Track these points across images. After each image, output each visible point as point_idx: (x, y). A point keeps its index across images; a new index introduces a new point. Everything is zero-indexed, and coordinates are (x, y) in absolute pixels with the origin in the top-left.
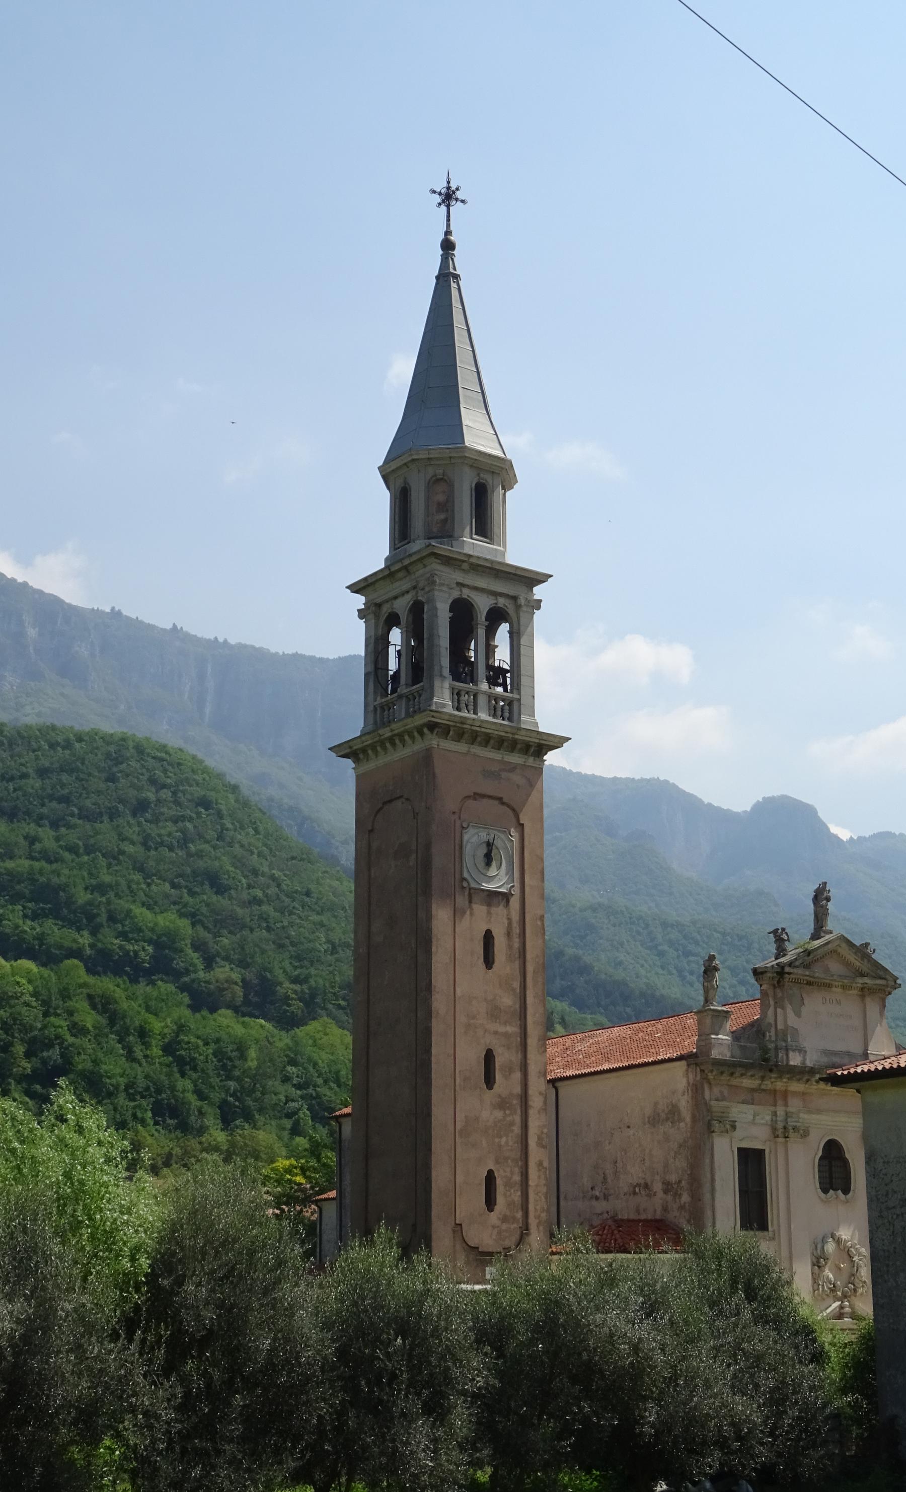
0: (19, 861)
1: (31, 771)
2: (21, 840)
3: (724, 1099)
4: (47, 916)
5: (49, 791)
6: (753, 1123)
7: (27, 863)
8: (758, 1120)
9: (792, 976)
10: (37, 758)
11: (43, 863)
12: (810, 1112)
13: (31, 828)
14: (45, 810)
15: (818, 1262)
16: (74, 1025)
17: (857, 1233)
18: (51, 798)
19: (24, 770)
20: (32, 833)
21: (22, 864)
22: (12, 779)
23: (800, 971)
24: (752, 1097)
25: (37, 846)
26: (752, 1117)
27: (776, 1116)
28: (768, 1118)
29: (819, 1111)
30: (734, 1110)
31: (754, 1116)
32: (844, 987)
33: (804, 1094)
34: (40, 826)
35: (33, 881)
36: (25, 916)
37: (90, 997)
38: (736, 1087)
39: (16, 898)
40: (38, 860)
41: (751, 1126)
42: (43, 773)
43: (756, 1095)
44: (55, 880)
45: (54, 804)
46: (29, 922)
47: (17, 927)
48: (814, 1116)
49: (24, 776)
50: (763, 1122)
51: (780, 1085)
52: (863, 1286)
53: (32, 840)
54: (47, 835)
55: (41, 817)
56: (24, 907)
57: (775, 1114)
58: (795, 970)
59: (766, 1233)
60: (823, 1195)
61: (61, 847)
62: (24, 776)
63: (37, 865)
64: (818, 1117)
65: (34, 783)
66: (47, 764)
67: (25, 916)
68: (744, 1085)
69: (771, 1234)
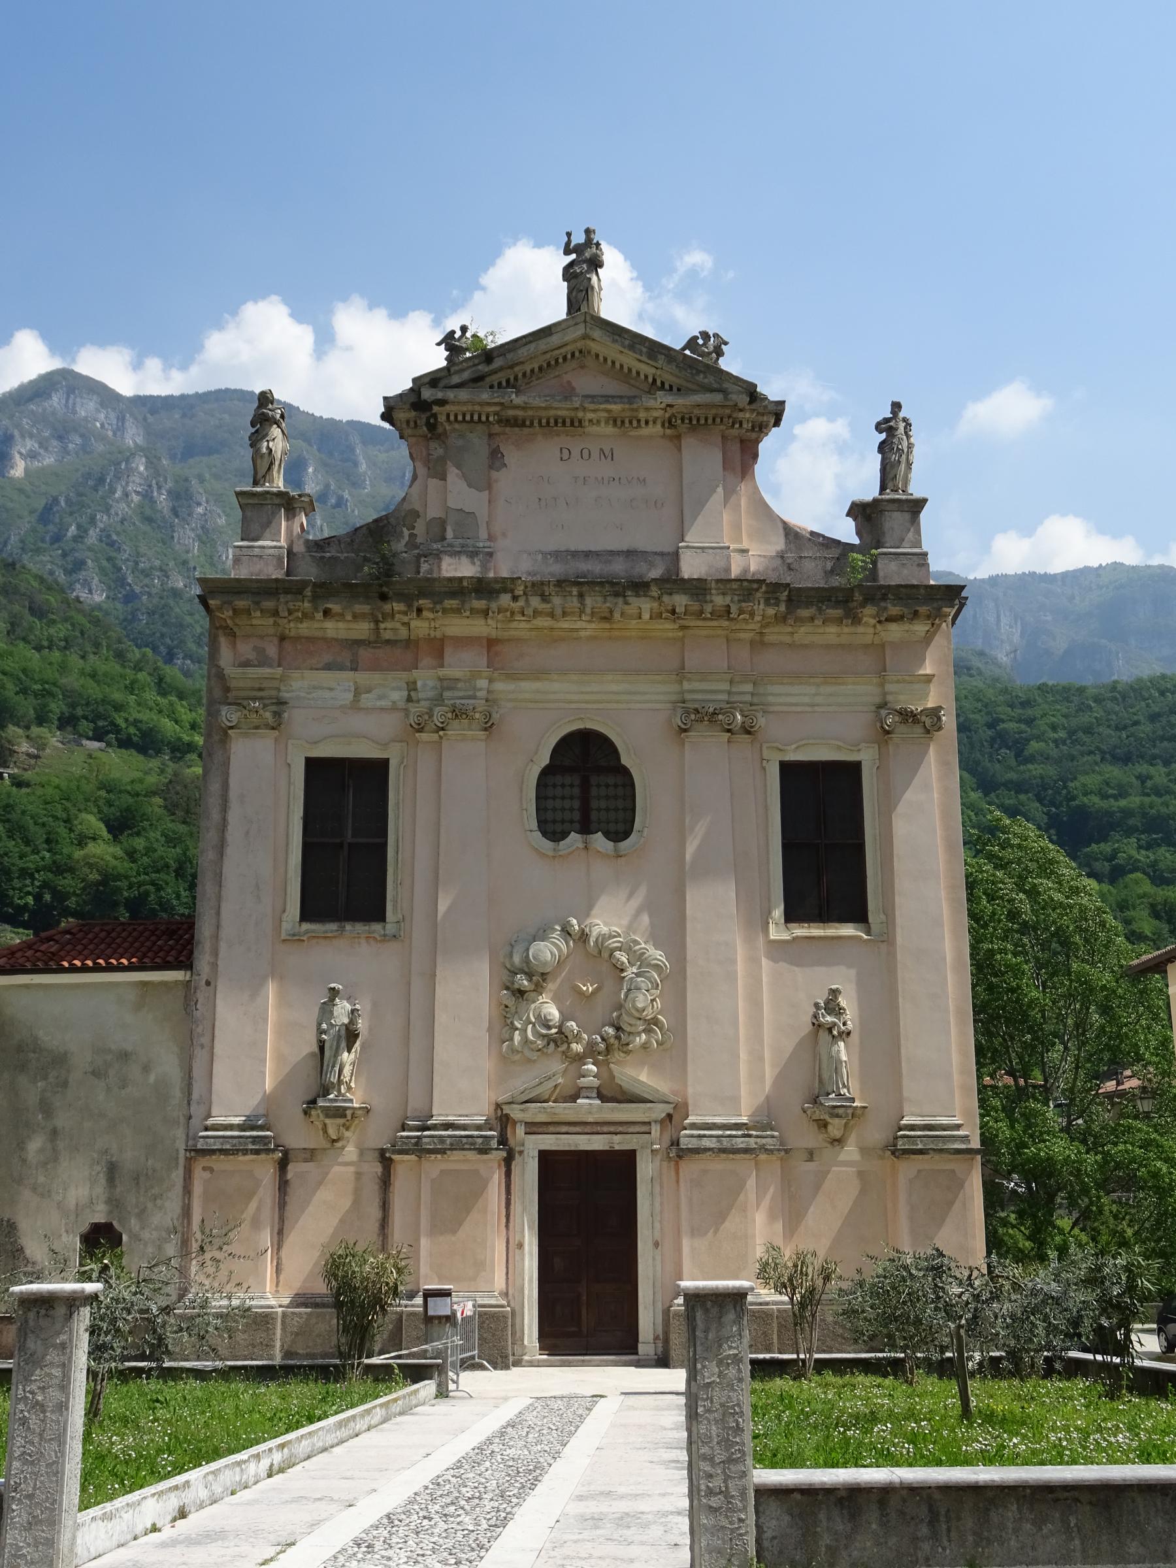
0: (1132, 798)
1: (1141, 718)
2: (1134, 780)
3: (263, 661)
4: (1159, 845)
5: (1160, 733)
6: (355, 706)
7: (1137, 800)
8: (367, 700)
9: (448, 408)
10: (1148, 705)
11: (1153, 797)
12: (512, 677)
13: (1143, 768)
14: (1156, 751)
15: (518, 984)
16: (1133, 933)
17: (645, 919)
18: (1163, 739)
19: (1136, 718)
20: (1144, 772)
21: (1134, 801)
22: (1125, 728)
23: (463, 394)
24: (350, 656)
25: (1149, 783)
26: (350, 696)
27: (415, 689)
28: (398, 696)
29: (538, 674)
30: (296, 685)
31: (357, 693)
32: (615, 421)
33: (491, 643)
34: (1152, 765)
35: (1145, 815)
36: (1140, 847)
37: (1153, 906)
38: (310, 639)
39: (1129, 832)
40: (1148, 795)
41: (342, 710)
42: (1154, 718)
43: (364, 654)
44: (1164, 810)
45: (1165, 743)
46: (1143, 852)
47: (1131, 857)
48: (526, 685)
49: (1136, 723)
50: (383, 703)
51: (420, 627)
52: (648, 1031)
53: (1142, 779)
54: (1159, 774)
55: (1154, 757)
56: (1139, 840)
57: (412, 686)
58: (450, 395)
59: (377, 927)
60: (547, 845)
61: (1170, 781)
62: (1136, 723)
63: (1147, 800)
64: (537, 685)
65: (1146, 728)
66: (1157, 710)
67: (1140, 847)
68: (330, 634)
69: (390, 928)
